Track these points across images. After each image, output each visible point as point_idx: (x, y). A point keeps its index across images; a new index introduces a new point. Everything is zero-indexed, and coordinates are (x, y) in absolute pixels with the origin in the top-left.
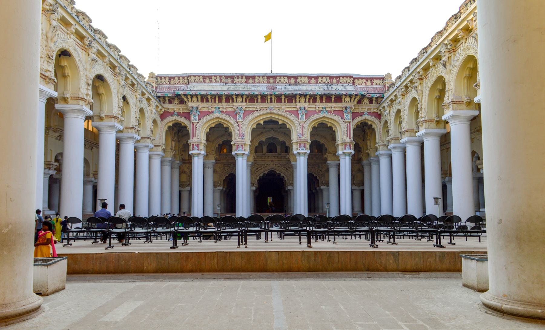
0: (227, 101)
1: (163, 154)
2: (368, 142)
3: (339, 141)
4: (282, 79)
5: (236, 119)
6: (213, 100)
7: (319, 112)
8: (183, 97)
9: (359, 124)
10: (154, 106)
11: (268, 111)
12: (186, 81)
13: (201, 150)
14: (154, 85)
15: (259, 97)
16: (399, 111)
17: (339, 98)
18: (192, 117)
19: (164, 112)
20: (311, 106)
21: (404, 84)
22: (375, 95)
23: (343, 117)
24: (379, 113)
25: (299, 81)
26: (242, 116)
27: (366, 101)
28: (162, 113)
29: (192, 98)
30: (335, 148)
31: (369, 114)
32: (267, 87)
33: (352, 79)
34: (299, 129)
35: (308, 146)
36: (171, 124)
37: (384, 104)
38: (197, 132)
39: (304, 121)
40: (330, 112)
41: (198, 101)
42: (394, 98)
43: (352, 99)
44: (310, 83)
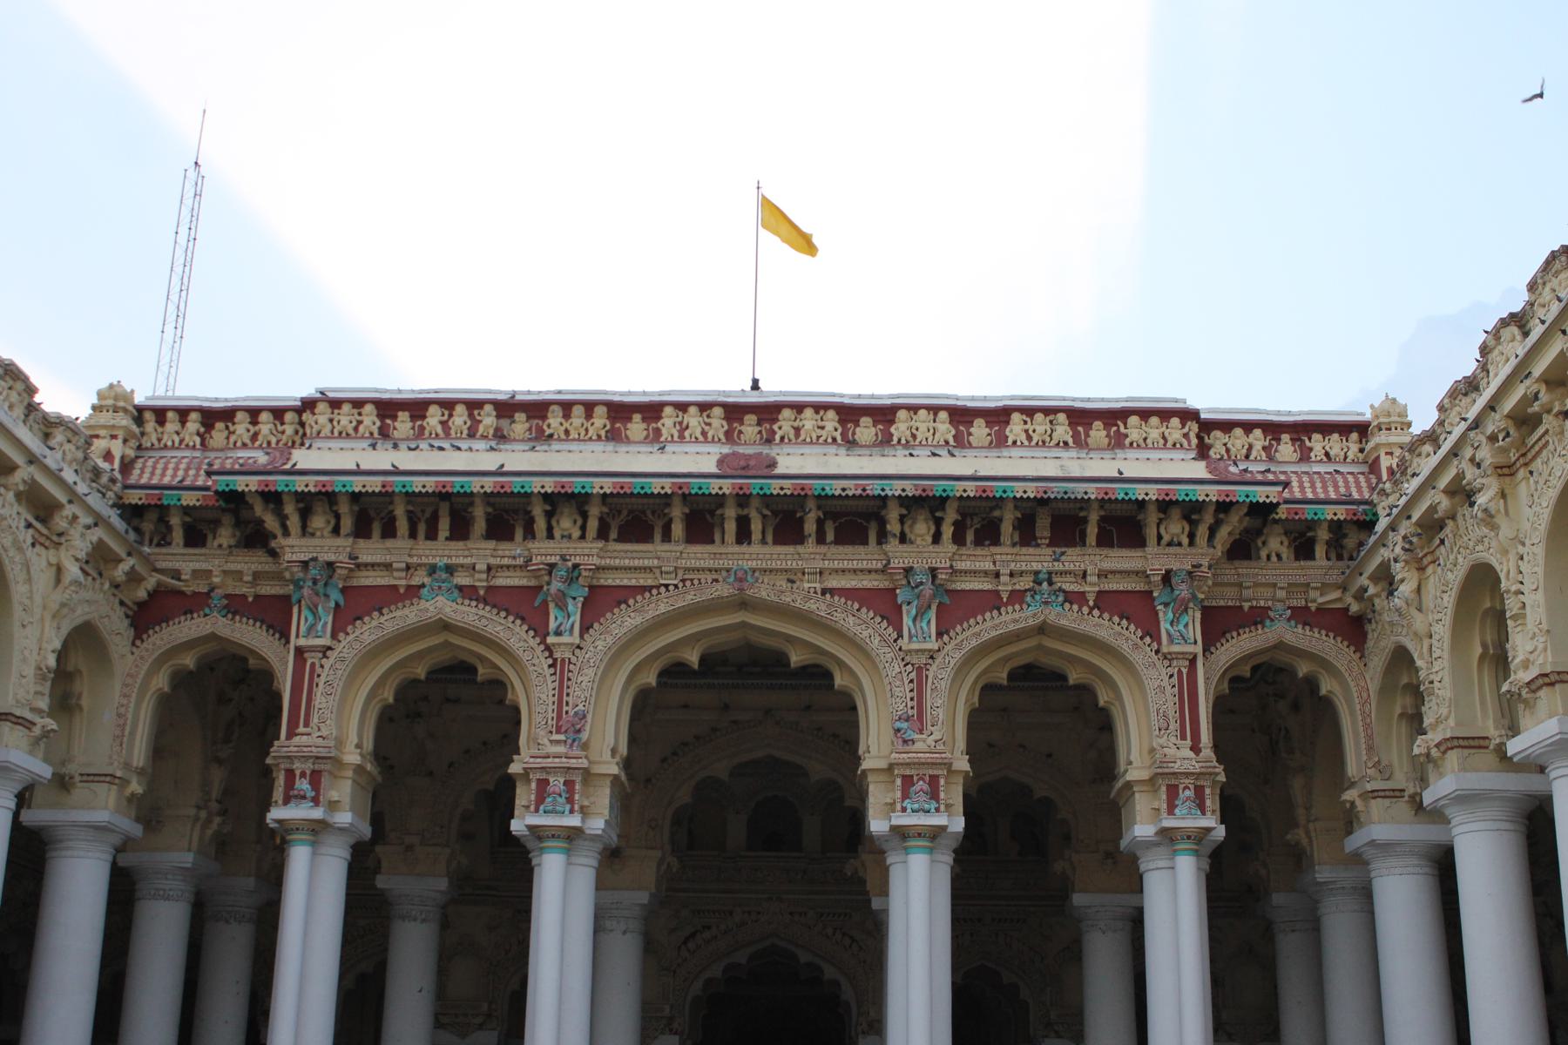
0: (499, 529)
1: (136, 830)
2: (1297, 783)
3: (1135, 764)
4: (809, 420)
5: (541, 631)
6: (422, 528)
7: (1017, 597)
8: (259, 509)
9: (1246, 671)
10: (80, 543)
11: (724, 590)
12: (289, 430)
13: (333, 806)
14: (117, 448)
15: (677, 512)
16: (1482, 580)
17: (1123, 521)
18: (300, 620)
19: (154, 594)
20: (976, 566)
21: (1509, 404)
22: (1328, 513)
23: (1151, 631)
24: (1355, 608)
25: (900, 429)
26: (576, 618)
27: (1276, 543)
28: (142, 594)
29: (305, 515)
30: (1114, 814)
31: (1301, 615)
32: (720, 462)
33: (1194, 427)
34: (904, 691)
35: (954, 795)
36: (189, 661)
37: (1385, 553)
38: (319, 700)
39: (933, 645)
40: (1073, 598)
41: (336, 531)
42: (1445, 503)
43: (1202, 532)
44: (961, 442)
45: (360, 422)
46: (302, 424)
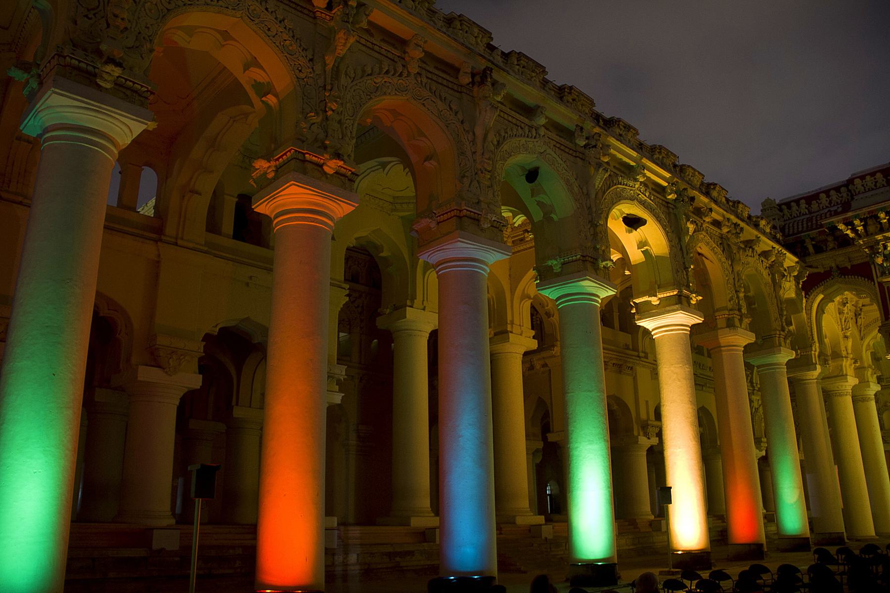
12: (845, 195)
45: (876, 182)
46: (849, 191)
